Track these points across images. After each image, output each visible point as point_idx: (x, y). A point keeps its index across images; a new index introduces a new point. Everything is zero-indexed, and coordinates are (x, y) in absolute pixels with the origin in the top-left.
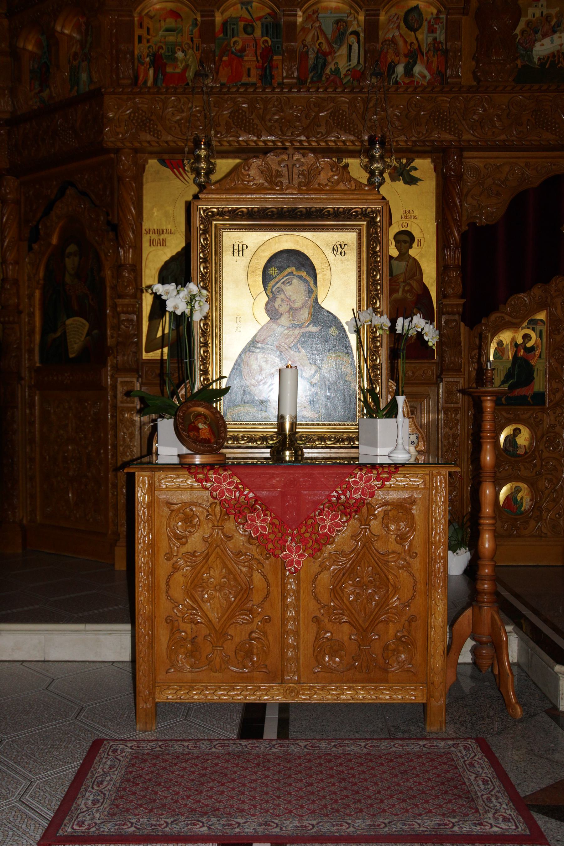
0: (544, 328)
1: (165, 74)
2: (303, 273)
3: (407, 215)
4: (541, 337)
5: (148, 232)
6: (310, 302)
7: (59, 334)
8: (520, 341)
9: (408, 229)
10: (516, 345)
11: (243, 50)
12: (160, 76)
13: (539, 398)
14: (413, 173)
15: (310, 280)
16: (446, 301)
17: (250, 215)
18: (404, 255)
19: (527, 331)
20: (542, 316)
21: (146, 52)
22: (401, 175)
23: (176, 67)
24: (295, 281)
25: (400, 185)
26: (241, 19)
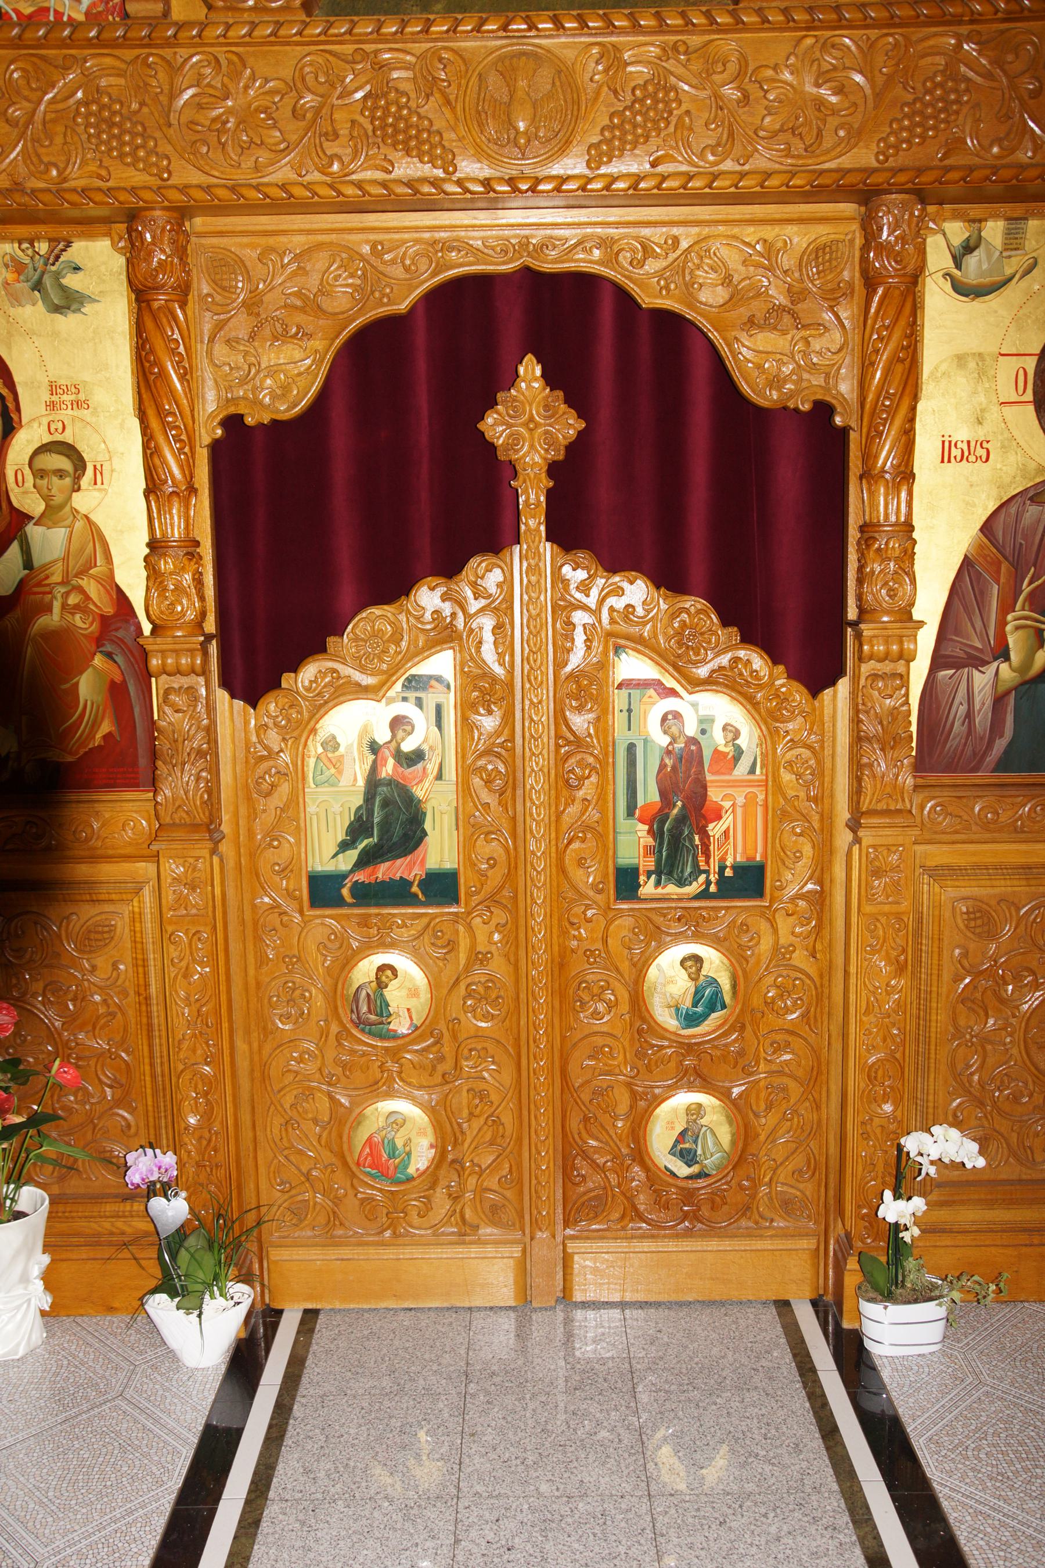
0: (450, 701)
4: (439, 724)
8: (383, 736)
9: (68, 437)
10: (374, 748)
14: (71, 281)
19: (408, 709)
22: (38, 286)
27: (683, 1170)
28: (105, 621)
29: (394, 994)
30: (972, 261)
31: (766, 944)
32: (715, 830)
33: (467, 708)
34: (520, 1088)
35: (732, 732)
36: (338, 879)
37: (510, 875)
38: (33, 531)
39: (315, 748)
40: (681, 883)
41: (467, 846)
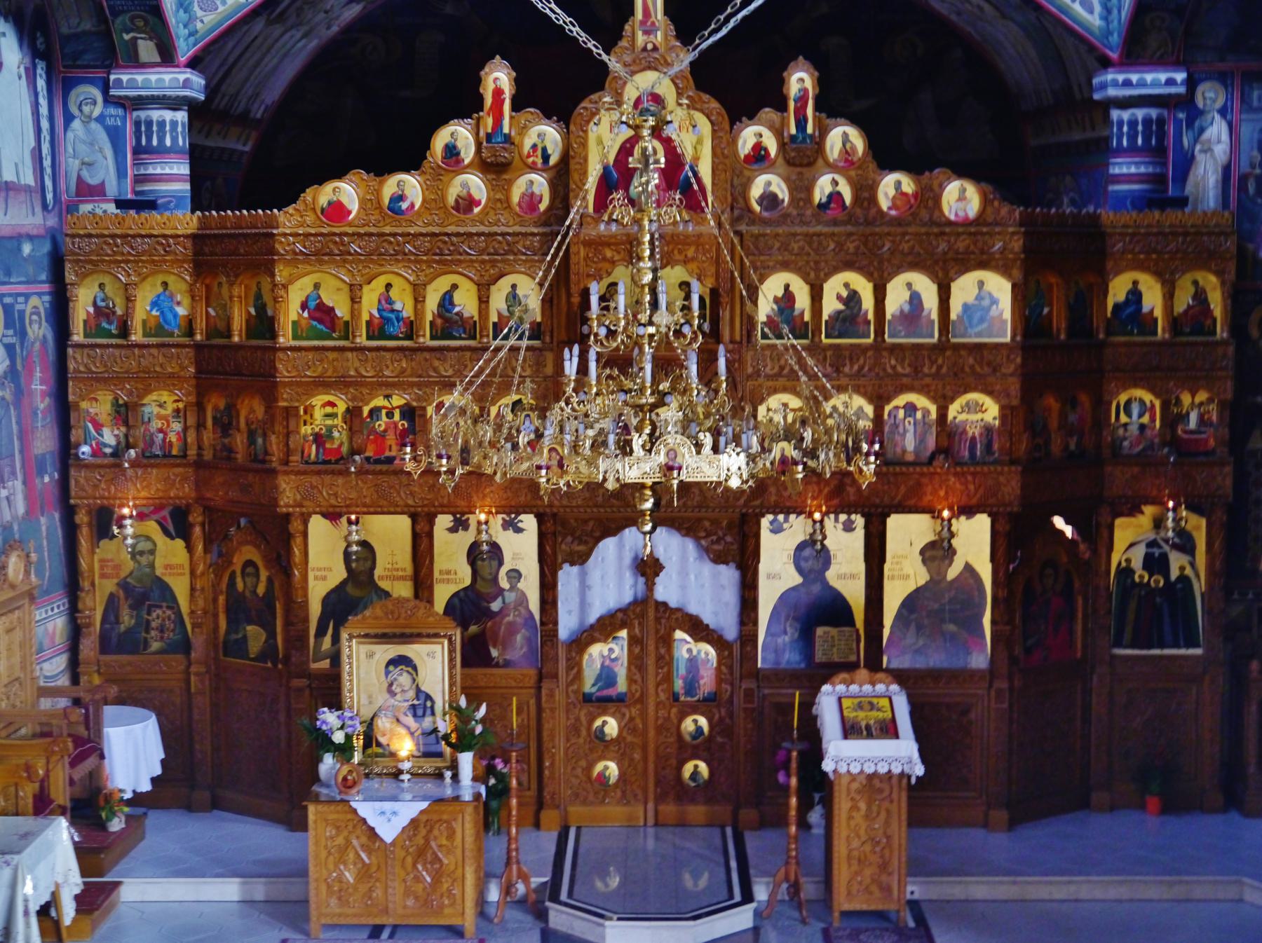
1: (325, 449)
2: (410, 669)
3: (516, 557)
4: (622, 649)
5: (313, 570)
6: (414, 686)
7: (240, 636)
8: (606, 653)
9: (517, 568)
10: (603, 657)
11: (385, 431)
12: (321, 450)
13: (620, 699)
14: (520, 525)
15: (414, 673)
16: (546, 628)
17: (376, 636)
18: (513, 588)
20: (624, 634)
21: (309, 431)
22: (511, 525)
23: (333, 443)
24: (405, 674)
25: (510, 532)
26: (384, 407)
27: (693, 784)
28: (526, 620)
29: (607, 730)
30: (775, 524)
31: (717, 716)
32: (702, 682)
33: (630, 645)
34: (645, 759)
35: (707, 654)
36: (591, 695)
37: (642, 695)
38: (506, 594)
39: (586, 657)
40: (692, 697)
41: (629, 685)
